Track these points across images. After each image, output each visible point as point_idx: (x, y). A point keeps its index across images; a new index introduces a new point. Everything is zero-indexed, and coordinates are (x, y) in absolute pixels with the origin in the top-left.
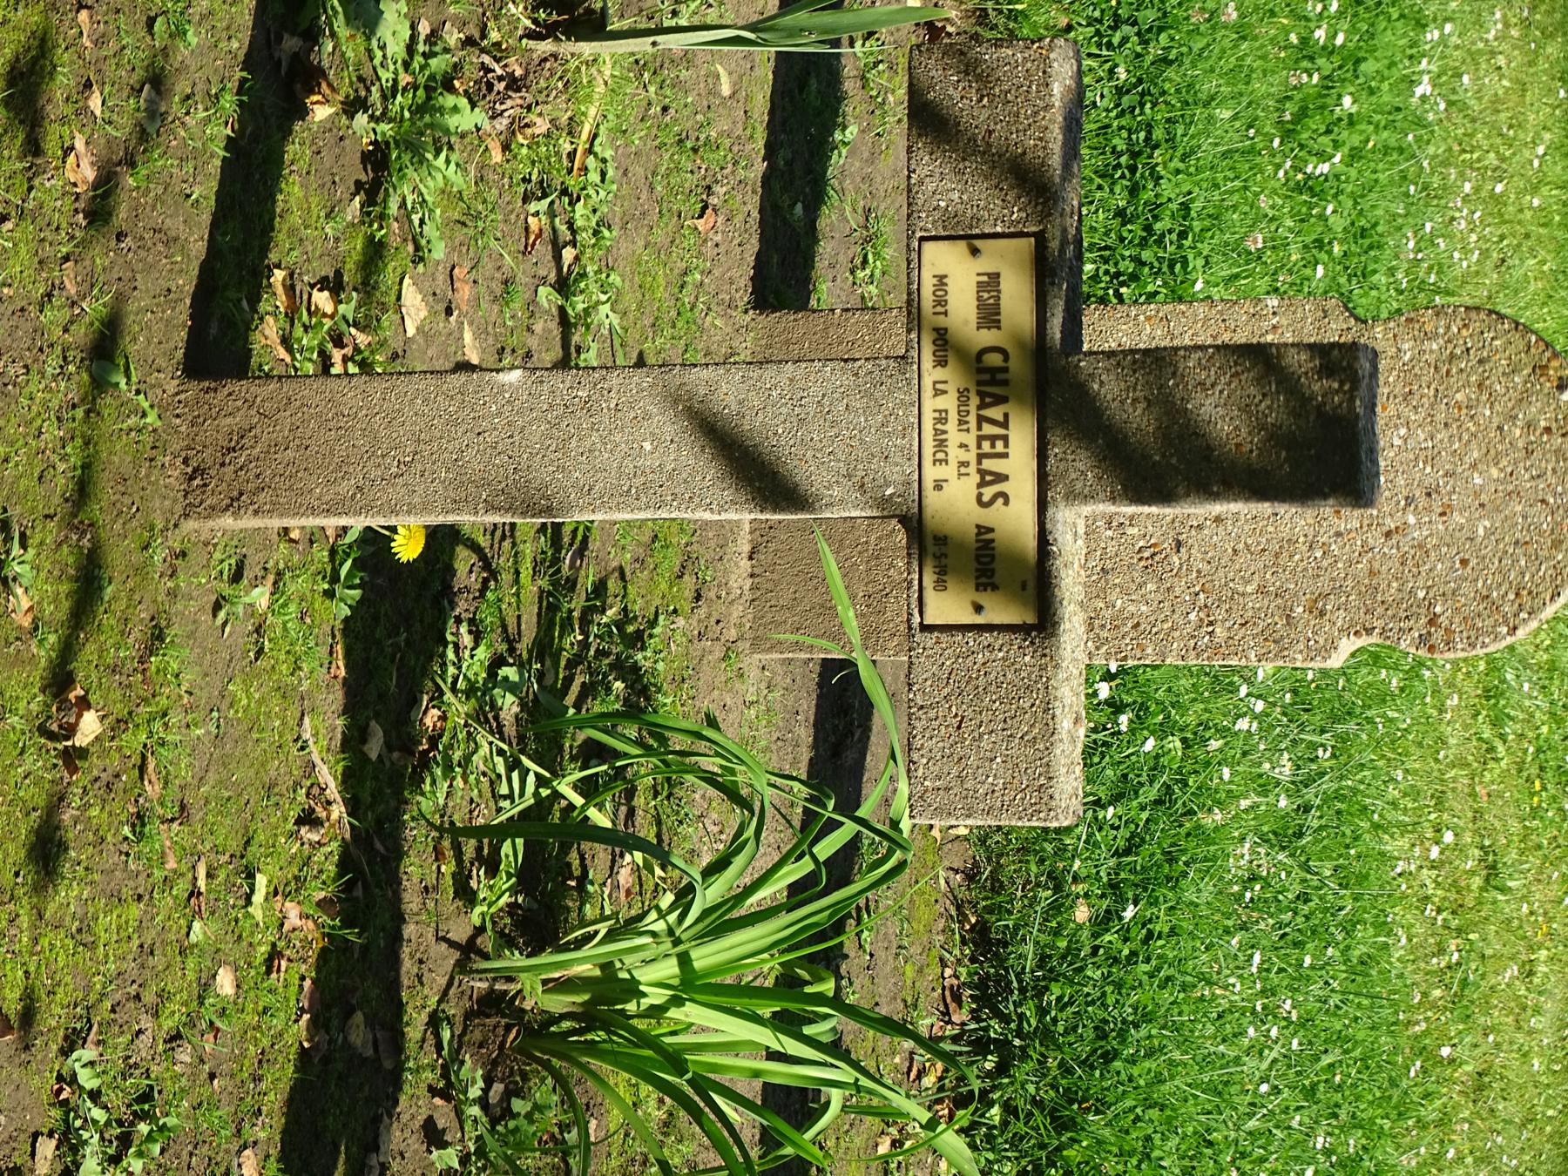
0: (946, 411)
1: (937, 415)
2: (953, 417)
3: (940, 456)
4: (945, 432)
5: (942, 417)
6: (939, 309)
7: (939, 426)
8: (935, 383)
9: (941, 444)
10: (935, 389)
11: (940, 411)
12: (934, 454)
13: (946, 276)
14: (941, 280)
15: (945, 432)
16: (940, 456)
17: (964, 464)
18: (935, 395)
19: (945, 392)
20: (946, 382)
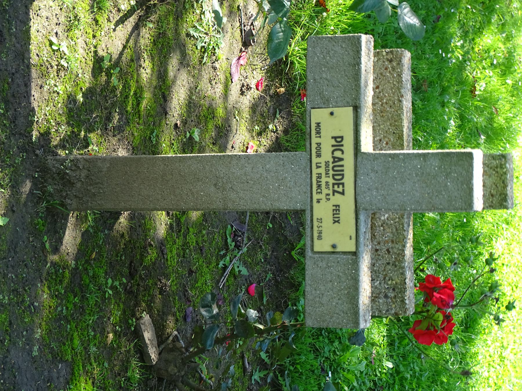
0: (321, 174)
1: (317, 175)
2: (323, 175)
3: (319, 191)
4: (320, 182)
5: (319, 176)
6: (318, 135)
7: (318, 180)
8: (317, 163)
9: (319, 186)
10: (317, 166)
11: (319, 174)
12: (317, 190)
13: (320, 123)
14: (318, 125)
15: (320, 182)
16: (319, 191)
17: (328, 195)
18: (317, 168)
19: (320, 167)
20: (320, 163)
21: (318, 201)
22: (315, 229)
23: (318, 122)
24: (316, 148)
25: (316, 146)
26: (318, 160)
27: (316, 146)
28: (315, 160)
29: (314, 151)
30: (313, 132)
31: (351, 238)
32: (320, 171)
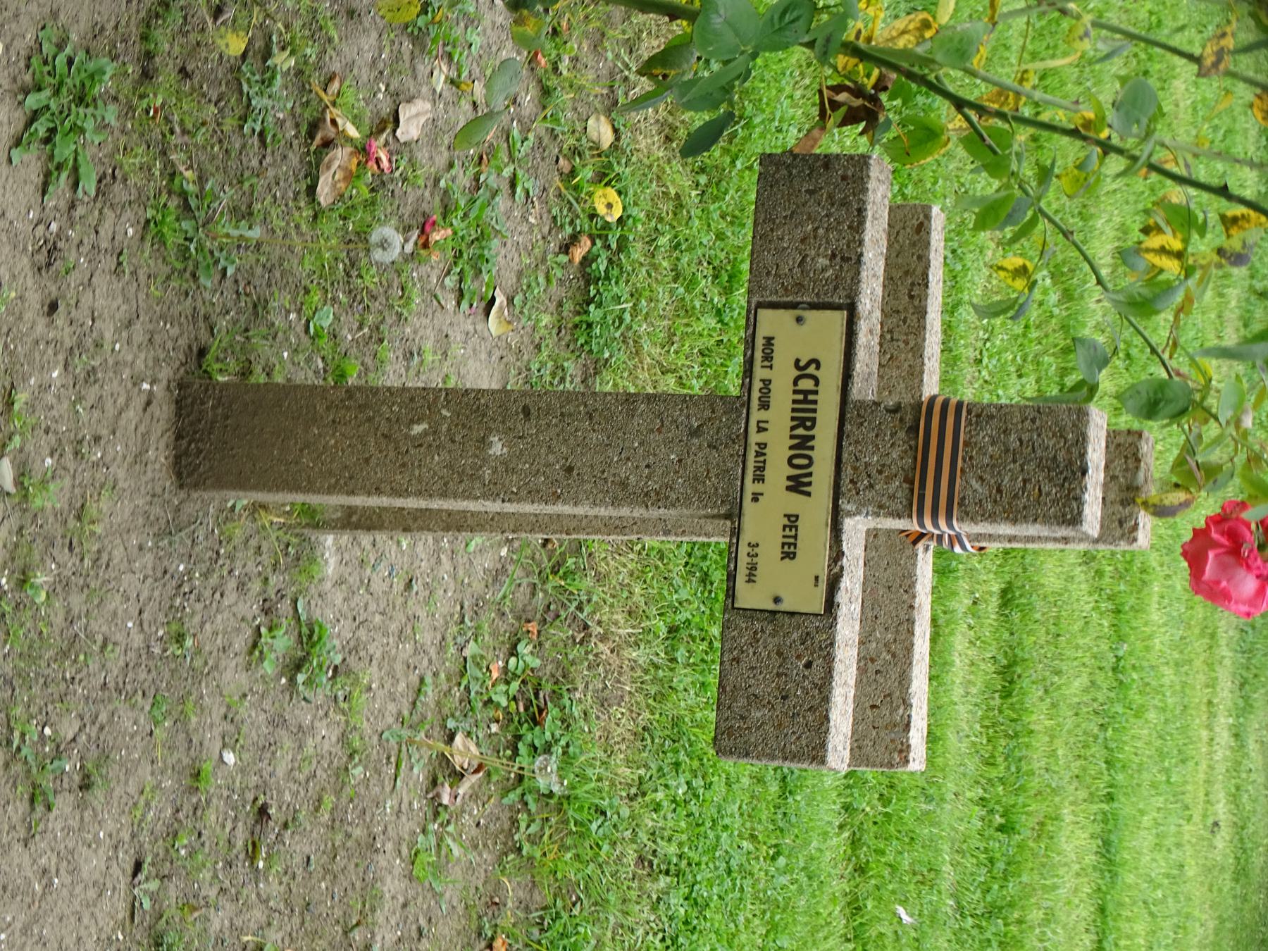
6: (766, 363)
9: (760, 468)
18: (758, 431)
19: (766, 430)
21: (755, 499)
22: (743, 560)
23: (770, 335)
24: (760, 390)
25: (761, 385)
26: (763, 415)
27: (761, 385)
28: (756, 415)
29: (756, 395)
30: (758, 355)
31: (817, 578)
32: (761, 438)
